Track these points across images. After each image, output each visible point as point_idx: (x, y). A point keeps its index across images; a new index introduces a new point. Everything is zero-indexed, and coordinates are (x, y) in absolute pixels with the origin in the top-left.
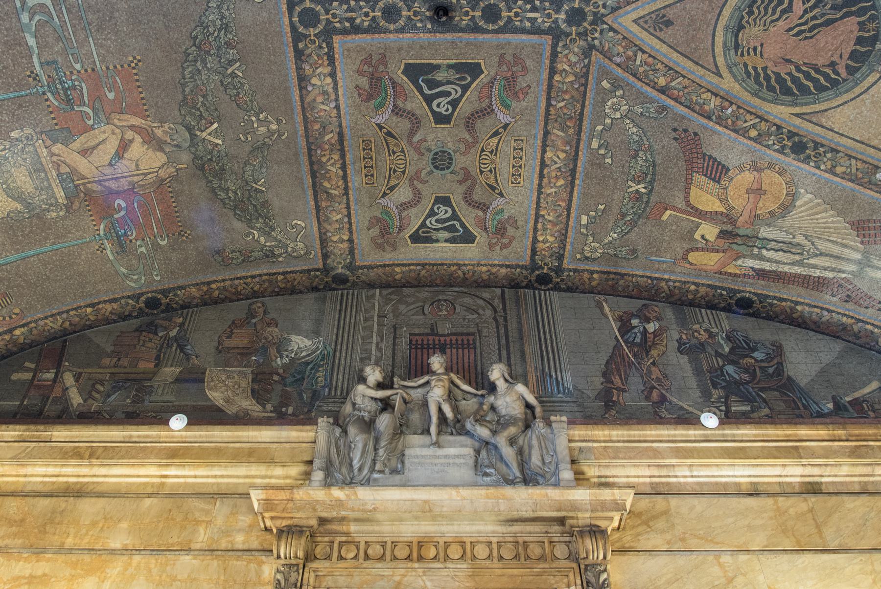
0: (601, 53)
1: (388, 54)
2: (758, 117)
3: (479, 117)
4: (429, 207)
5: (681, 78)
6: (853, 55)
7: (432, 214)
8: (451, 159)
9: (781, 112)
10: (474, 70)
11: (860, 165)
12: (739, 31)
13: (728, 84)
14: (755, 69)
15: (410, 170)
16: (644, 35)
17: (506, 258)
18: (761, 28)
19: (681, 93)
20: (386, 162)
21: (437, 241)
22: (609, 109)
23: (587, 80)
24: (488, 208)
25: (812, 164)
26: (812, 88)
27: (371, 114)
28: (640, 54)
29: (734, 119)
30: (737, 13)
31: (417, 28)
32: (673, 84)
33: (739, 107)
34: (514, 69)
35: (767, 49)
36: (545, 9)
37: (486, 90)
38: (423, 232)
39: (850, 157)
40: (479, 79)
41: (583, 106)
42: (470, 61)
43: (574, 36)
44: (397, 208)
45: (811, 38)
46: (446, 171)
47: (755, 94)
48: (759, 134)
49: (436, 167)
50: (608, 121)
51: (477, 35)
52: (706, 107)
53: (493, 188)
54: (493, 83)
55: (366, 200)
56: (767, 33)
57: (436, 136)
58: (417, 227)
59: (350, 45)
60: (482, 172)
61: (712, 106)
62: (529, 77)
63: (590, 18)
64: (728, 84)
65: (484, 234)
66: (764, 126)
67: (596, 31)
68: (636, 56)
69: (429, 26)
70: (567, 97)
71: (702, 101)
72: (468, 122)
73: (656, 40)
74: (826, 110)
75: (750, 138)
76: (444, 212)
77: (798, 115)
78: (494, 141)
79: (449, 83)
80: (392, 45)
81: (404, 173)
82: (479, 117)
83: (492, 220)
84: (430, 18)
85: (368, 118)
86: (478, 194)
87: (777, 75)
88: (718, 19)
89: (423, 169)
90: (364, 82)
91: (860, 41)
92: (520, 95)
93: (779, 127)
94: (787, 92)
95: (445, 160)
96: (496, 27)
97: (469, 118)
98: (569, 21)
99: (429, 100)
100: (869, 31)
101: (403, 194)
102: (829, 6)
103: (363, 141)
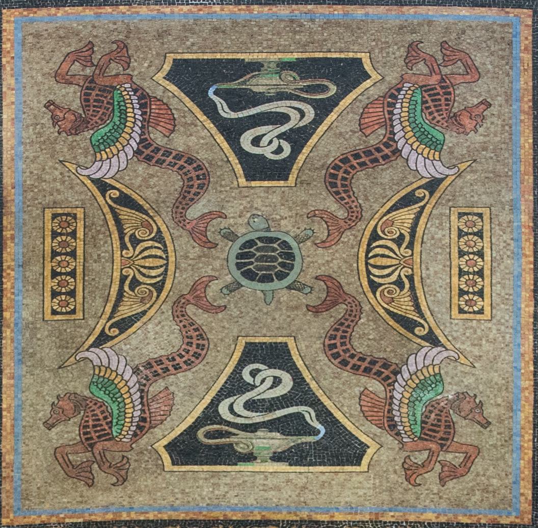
3: (363, 164)
4: (229, 370)
7: (235, 386)
8: (291, 256)
15: (179, 281)
17: (458, 504)
20: (110, 262)
21: (250, 457)
24: (397, 372)
27: (82, 160)
34: (445, 71)
37: (377, 111)
38: (208, 435)
44: (136, 371)
46: (276, 284)
49: (250, 275)
51: (350, 8)
53: (409, 325)
54: (394, 97)
55: (49, 353)
57: (246, 207)
58: (190, 421)
59: (41, 26)
60: (374, 286)
65: (388, 439)
72: (334, 176)
76: (268, 383)
78: (406, 216)
80: (144, 26)
81: (159, 287)
82: (363, 164)
83: (412, 403)
85: (72, 168)
86: (367, 338)
89: (212, 278)
90: (70, 96)
92: (466, 121)
95: (274, 259)
97: (337, 168)
99: (232, 131)
101: (157, 336)
103: (55, 216)
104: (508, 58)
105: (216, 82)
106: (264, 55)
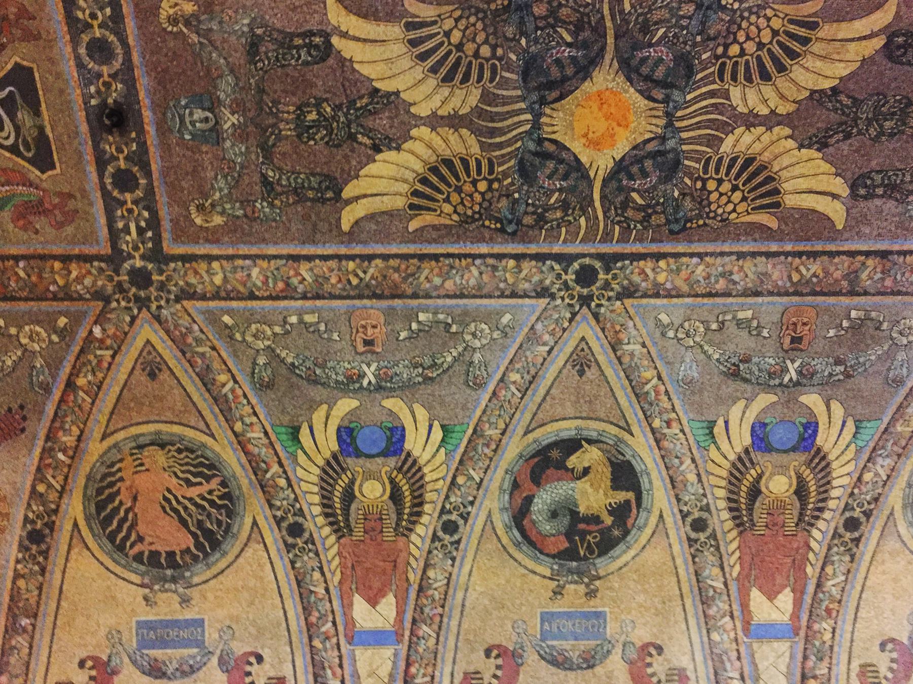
0: (102, 311)
1: (41, 42)
2: (63, 487)
5: (90, 400)
6: (155, 555)
9: (74, 508)
10: (44, 161)
11: (33, 601)
12: (158, 445)
13: (95, 449)
14: (120, 470)
16: (134, 353)
18: (166, 465)
19: (71, 404)
22: (31, 330)
23: (62, 300)
25: (20, 556)
26: (110, 529)
28: (110, 352)
29: (54, 464)
30: (177, 439)
31: (87, 85)
32: (81, 393)
33: (70, 466)
34: (57, 212)
35: (143, 476)
36: (143, 243)
39: (40, 588)
40: (31, 168)
41: (26, 299)
42: (55, 157)
43: (116, 278)
45: (165, 512)
47: (89, 478)
48: (41, 495)
50: (13, 331)
52: (61, 433)
56: (162, 471)
61: (64, 439)
62: (51, 232)
63: (142, 294)
64: (95, 449)
66: (53, 496)
67: (129, 302)
68: (107, 349)
69: (93, 102)
70: (34, 278)
71: (67, 426)
73: (130, 366)
74: (88, 549)
75: (33, 487)
77: (76, 525)
79: (17, 129)
84: (104, 104)
87: (118, 492)
88: (166, 422)
91: (171, 555)
92: (21, 222)
93: (56, 511)
94: (100, 507)
96: (109, 187)
98: (133, 272)
100: (181, 558)
102: (200, 517)
104: (73, 242)
105: (19, 90)
106: (46, 117)
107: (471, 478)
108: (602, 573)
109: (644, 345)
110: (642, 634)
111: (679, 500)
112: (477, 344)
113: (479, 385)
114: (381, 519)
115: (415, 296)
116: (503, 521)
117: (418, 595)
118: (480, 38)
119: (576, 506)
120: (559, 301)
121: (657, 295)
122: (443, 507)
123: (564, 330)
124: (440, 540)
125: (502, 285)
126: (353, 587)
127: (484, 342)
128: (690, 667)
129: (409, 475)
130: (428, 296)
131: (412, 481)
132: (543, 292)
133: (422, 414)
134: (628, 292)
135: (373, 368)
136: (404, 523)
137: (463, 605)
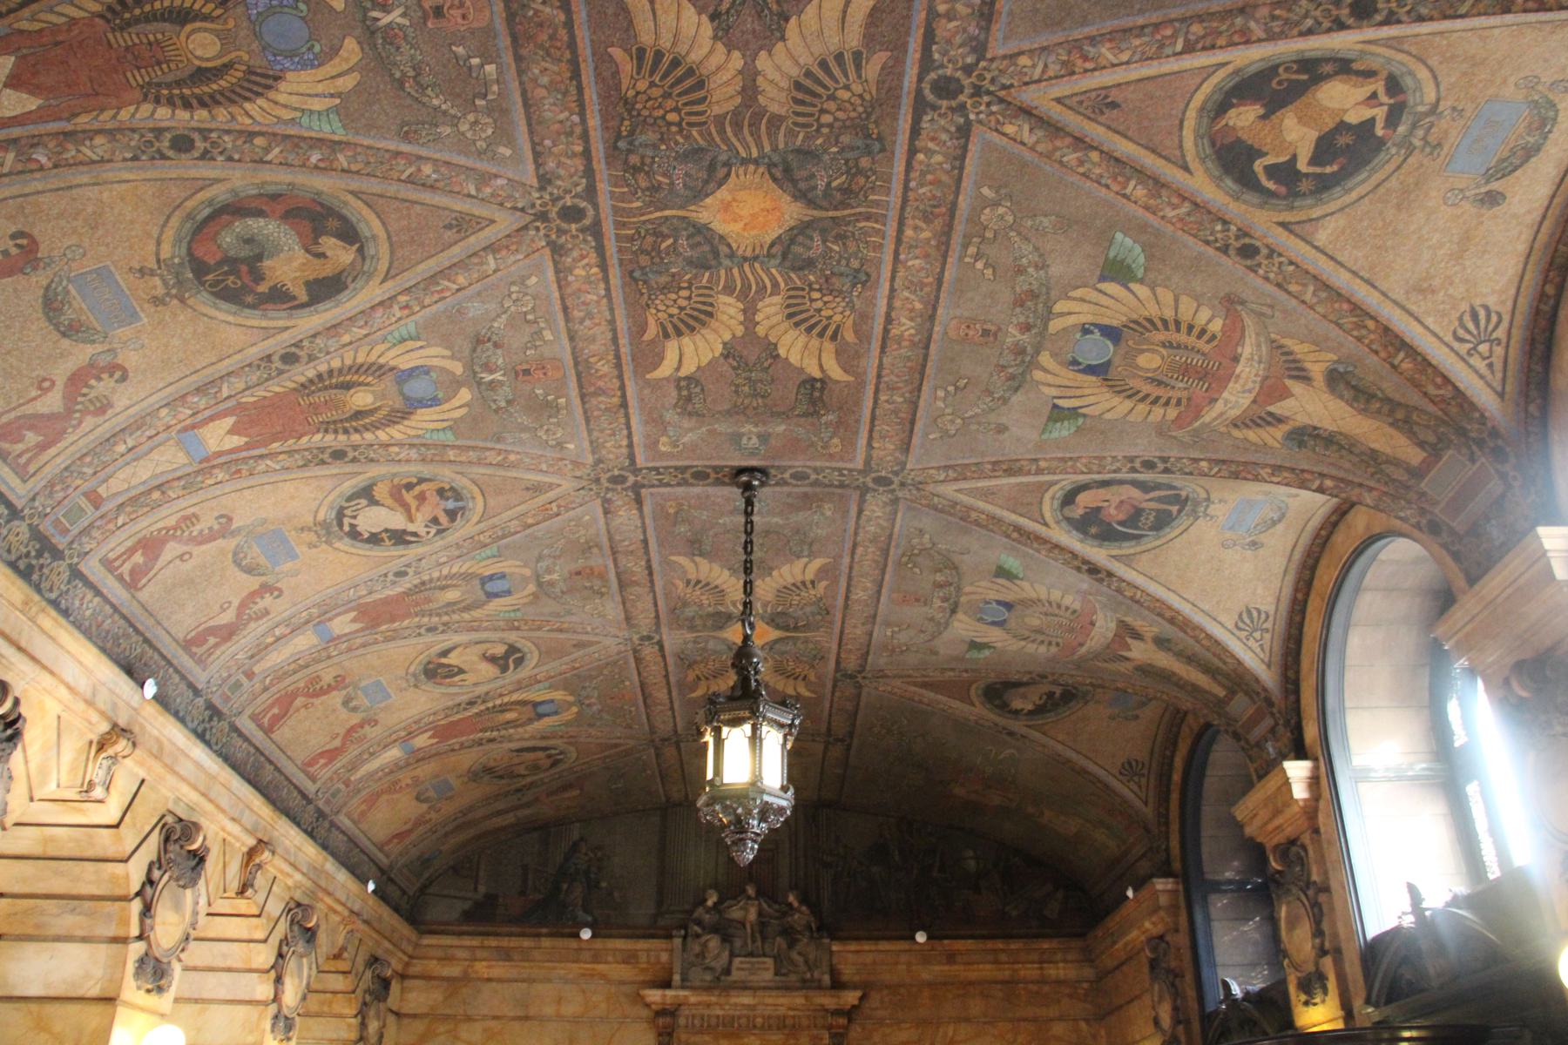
107: (267, 150)
108: (191, 302)
109: (495, 271)
110: (130, 359)
111: (314, 336)
112: (464, 127)
113: (406, 137)
114: (159, 63)
115: (518, 59)
116: (217, 196)
117: (58, 134)
118: (840, 115)
119: (271, 256)
120: (537, 195)
121: (557, 271)
122: (211, 131)
123: (501, 204)
124: (157, 138)
125: (547, 142)
126: (24, 51)
127: (469, 135)
128: (118, 410)
129: (246, 84)
130: (520, 72)
131: (238, 90)
132: (545, 181)
133: (348, 83)
134: (557, 250)
135: (399, 20)
136: (165, 92)
137: (70, 187)
